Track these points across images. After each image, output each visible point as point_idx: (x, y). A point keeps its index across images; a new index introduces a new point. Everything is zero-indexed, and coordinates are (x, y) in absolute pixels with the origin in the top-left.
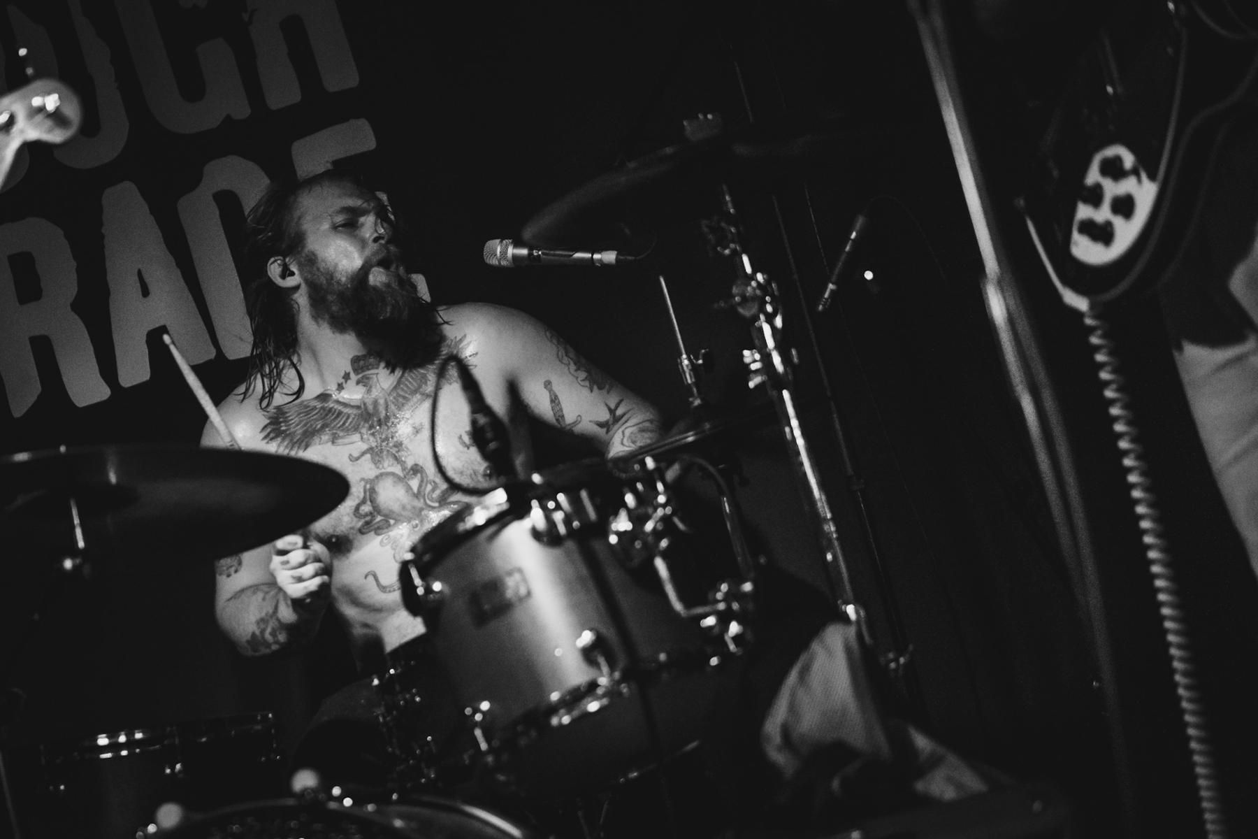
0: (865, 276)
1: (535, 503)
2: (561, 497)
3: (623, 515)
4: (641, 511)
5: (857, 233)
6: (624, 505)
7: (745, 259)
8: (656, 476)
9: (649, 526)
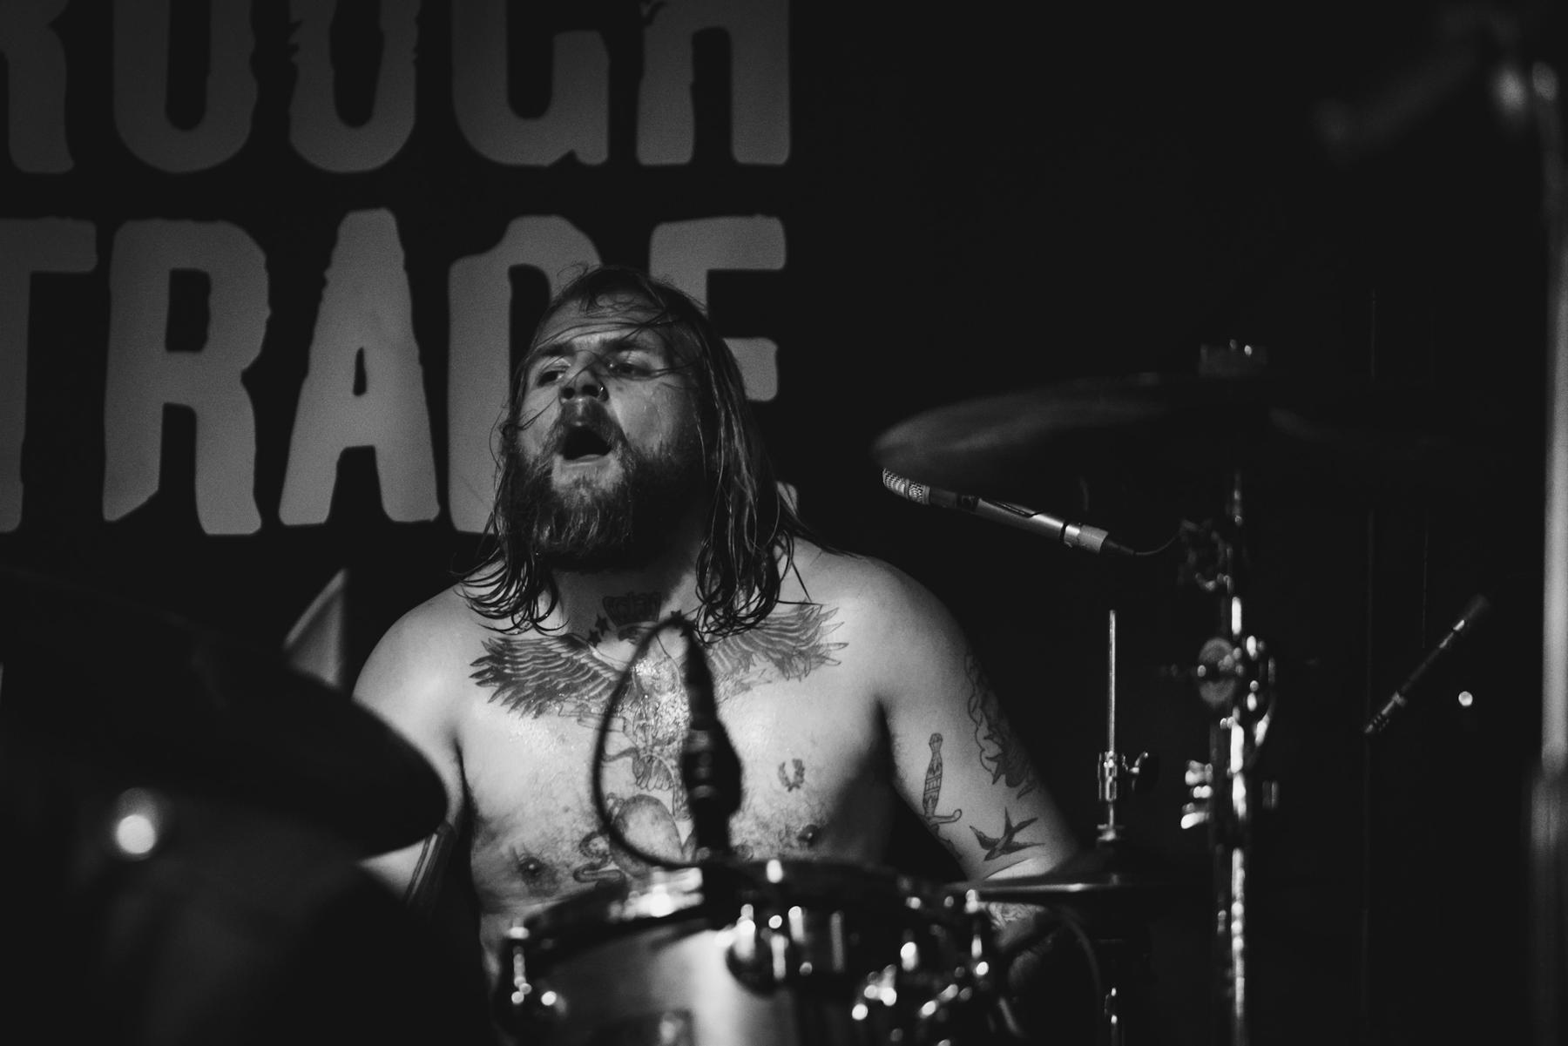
0: (1460, 698)
1: (747, 911)
2: (796, 914)
3: (889, 974)
4: (922, 979)
5: (1466, 623)
6: (897, 960)
7: (1236, 608)
8: (976, 926)
9: (929, 1009)
